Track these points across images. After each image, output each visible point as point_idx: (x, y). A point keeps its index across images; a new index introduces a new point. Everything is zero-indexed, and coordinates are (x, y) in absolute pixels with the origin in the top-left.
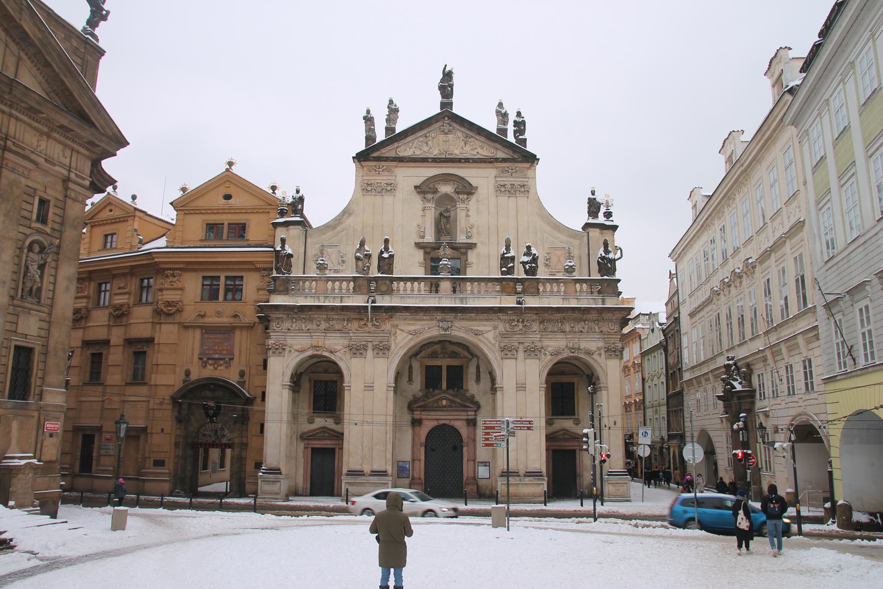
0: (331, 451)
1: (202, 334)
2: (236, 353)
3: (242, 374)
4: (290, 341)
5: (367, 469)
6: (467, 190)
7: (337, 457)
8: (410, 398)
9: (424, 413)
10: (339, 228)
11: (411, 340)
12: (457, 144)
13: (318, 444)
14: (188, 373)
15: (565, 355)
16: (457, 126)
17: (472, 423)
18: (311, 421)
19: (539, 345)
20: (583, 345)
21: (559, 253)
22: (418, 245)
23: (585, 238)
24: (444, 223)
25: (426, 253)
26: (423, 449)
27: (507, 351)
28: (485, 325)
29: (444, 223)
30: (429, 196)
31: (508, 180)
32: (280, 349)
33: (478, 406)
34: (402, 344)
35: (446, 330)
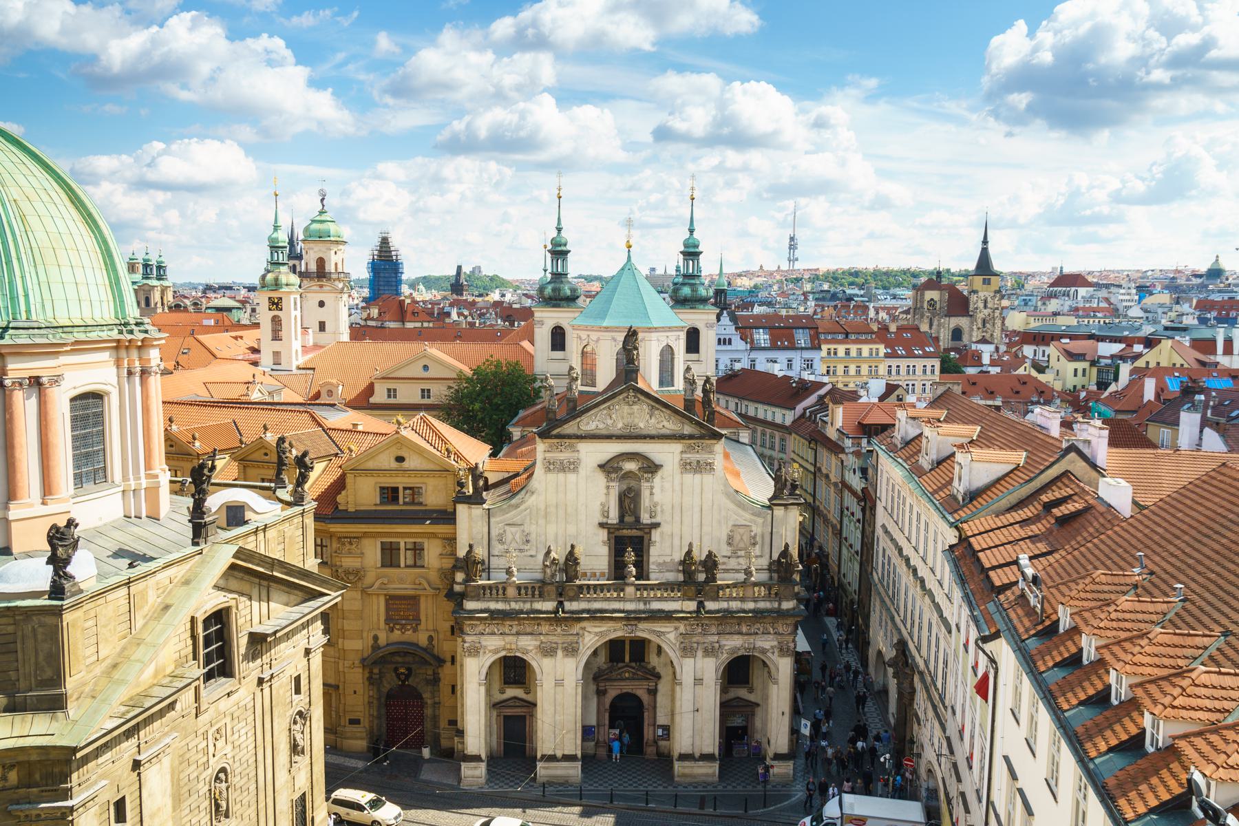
1: (387, 601)
2: (423, 618)
3: (431, 638)
4: (484, 643)
5: (559, 754)
6: (652, 468)
8: (595, 670)
10: (522, 507)
12: (642, 417)
13: (509, 712)
14: (376, 638)
15: (740, 654)
16: (642, 398)
17: (653, 692)
18: (502, 692)
21: (741, 530)
22: (602, 525)
23: (769, 517)
24: (629, 501)
25: (609, 533)
26: (607, 715)
27: (687, 651)
29: (629, 501)
30: (613, 475)
31: (693, 457)
32: (475, 651)
33: (658, 677)
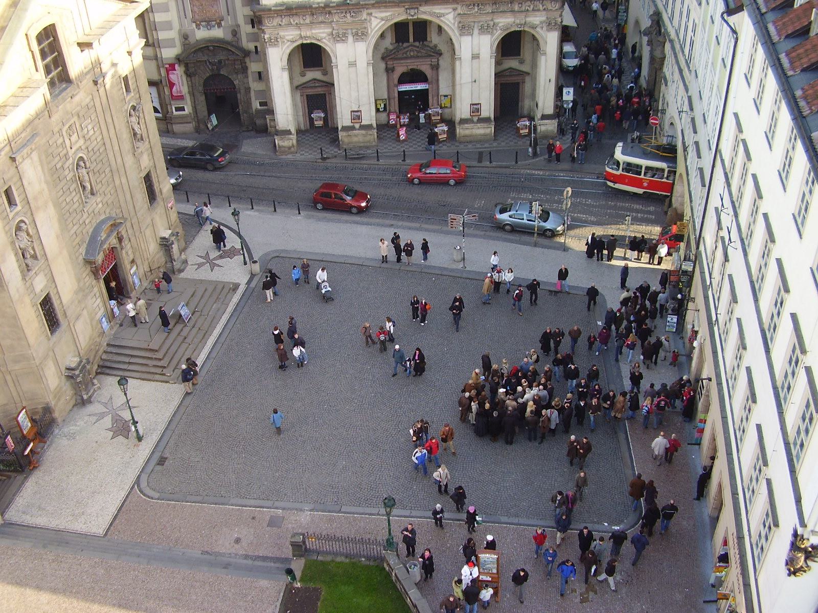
0: (323, 97)
4: (282, 33)
7: (327, 99)
8: (383, 50)
9: (395, 62)
11: (383, 25)
13: (311, 92)
15: (513, 29)
17: (436, 68)
18: (303, 75)
19: (492, 23)
20: (529, 19)
27: (465, 29)
28: (446, 8)
32: (275, 42)
33: (441, 54)
34: (376, 29)
35: (412, 16)
